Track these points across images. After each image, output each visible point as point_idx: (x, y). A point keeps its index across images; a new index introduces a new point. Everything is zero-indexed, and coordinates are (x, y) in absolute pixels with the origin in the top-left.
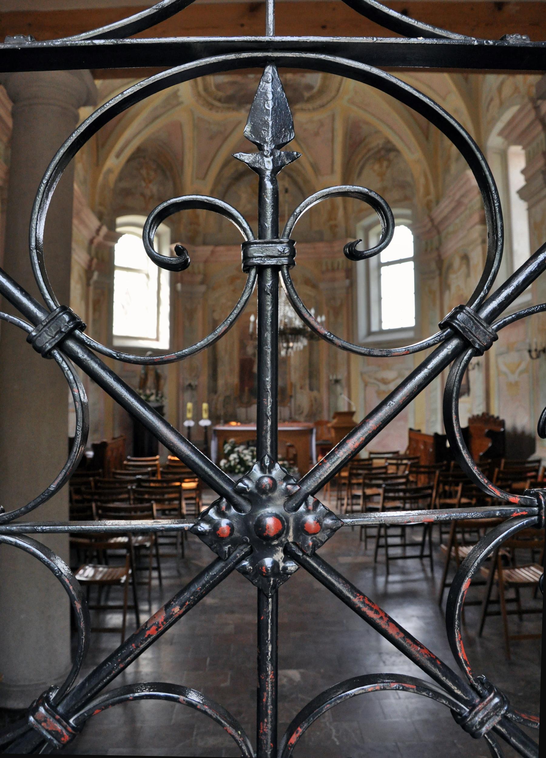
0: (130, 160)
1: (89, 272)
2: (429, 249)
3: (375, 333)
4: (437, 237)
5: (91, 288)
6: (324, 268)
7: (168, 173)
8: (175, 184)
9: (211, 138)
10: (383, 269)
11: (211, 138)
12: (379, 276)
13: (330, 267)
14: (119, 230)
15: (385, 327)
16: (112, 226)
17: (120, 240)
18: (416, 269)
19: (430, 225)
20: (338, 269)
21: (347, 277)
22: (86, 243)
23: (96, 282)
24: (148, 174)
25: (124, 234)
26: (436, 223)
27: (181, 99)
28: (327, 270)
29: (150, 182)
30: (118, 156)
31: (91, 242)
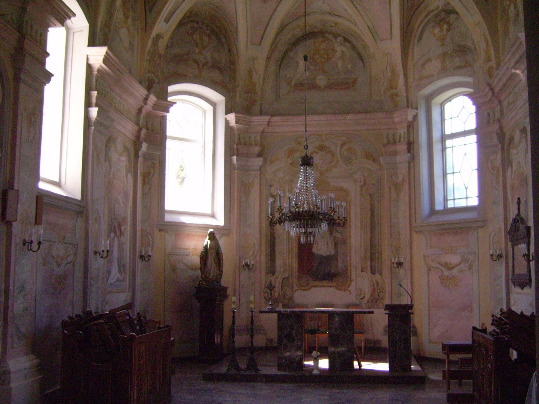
1: (137, 142)
2: (491, 121)
3: (439, 212)
4: (498, 109)
5: (140, 159)
6: (385, 141)
7: (223, 40)
8: (229, 50)
12: (444, 149)
13: (391, 141)
14: (169, 99)
15: (450, 205)
16: (163, 95)
17: (172, 109)
18: (479, 142)
19: (490, 94)
20: (400, 142)
21: (409, 151)
22: (134, 113)
23: (145, 154)
24: (201, 39)
25: (175, 103)
26: (497, 90)
28: (389, 142)
29: (204, 48)
30: (167, 21)
31: (140, 111)
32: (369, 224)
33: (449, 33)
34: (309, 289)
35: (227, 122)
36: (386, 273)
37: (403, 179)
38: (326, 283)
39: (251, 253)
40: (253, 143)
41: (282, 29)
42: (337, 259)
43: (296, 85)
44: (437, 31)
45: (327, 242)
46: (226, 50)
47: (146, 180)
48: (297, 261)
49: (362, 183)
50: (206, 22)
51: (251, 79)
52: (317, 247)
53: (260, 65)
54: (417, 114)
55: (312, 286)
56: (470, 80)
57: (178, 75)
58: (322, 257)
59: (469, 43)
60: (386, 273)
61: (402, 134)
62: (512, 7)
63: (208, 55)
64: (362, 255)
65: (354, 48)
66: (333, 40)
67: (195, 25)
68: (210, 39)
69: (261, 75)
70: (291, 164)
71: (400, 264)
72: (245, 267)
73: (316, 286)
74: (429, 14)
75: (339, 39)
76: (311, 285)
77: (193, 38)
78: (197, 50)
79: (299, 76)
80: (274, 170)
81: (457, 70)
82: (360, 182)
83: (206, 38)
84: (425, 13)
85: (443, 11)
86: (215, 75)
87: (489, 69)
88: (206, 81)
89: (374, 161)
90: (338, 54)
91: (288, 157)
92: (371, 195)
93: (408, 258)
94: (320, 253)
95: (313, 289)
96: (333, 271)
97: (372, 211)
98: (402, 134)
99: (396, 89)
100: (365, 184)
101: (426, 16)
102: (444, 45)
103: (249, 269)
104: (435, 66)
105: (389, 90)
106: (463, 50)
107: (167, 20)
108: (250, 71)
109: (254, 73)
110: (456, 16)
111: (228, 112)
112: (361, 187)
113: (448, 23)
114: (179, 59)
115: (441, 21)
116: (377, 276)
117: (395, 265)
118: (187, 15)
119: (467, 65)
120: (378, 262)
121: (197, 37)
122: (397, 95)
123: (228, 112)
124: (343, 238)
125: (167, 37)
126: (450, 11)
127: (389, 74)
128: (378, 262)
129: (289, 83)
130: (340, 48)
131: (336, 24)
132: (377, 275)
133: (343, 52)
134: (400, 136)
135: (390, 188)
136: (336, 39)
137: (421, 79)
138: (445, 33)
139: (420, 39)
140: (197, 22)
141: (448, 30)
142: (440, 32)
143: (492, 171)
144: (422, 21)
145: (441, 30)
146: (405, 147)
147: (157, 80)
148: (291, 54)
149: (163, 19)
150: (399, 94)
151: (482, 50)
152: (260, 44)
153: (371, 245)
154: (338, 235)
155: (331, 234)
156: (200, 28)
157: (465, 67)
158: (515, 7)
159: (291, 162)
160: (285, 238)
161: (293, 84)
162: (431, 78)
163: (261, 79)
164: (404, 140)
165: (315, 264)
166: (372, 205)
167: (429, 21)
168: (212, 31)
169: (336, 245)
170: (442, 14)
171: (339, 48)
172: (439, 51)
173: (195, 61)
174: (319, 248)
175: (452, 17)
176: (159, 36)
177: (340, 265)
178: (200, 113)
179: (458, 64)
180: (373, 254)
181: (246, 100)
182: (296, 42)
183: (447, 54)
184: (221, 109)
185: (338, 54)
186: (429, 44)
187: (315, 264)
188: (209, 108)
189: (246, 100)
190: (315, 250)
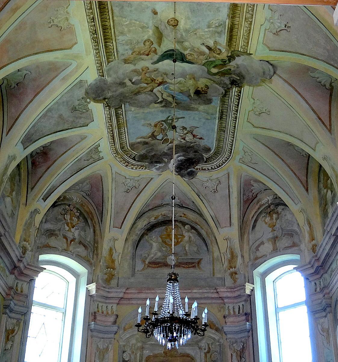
0: (54, 205)
2: (318, 290)
7: (89, 221)
8: (94, 232)
9: (127, 192)
10: (281, 314)
11: (127, 192)
24: (71, 219)
27: (101, 155)
30: (45, 199)
33: (278, 220)
35: (88, 291)
37: (243, 346)
40: (110, 312)
41: (140, 216)
43: (150, 263)
44: (268, 219)
46: (92, 230)
47: (10, 336)
50: (77, 206)
51: (112, 256)
53: (119, 245)
54: (254, 288)
56: (297, 257)
57: (50, 247)
59: (295, 228)
61: (241, 306)
62: (329, 192)
63: (76, 233)
65: (200, 234)
66: (182, 227)
67: (67, 207)
68: (78, 221)
69: (120, 253)
74: (261, 206)
75: (187, 227)
77: (64, 218)
78: (67, 228)
79: (152, 255)
81: (286, 250)
83: (75, 219)
84: (257, 207)
85: (272, 204)
86: (81, 250)
87: (313, 247)
88: (73, 255)
89: (217, 330)
90: (186, 238)
98: (241, 306)
99: (235, 268)
100: (208, 352)
101: (259, 209)
102: (275, 231)
104: (268, 247)
105: (230, 270)
106: (291, 234)
107: (45, 198)
108: (111, 250)
109: (114, 251)
110: (282, 207)
111: (89, 282)
113: (277, 213)
114: (51, 233)
115: (271, 212)
118: (61, 199)
119: (294, 245)
121: (68, 217)
122: (236, 273)
123: (89, 282)
125: (43, 212)
126: (279, 203)
127: (229, 256)
129: (144, 262)
130: (187, 235)
131: (184, 214)
133: (190, 237)
136: (184, 227)
137: (256, 259)
138: (274, 221)
139: (254, 227)
140: (69, 205)
141: (277, 219)
142: (270, 220)
143: (322, 333)
144: (256, 212)
145: (272, 219)
146: (244, 318)
147: (30, 249)
148: (146, 237)
149: (42, 197)
150: (238, 273)
151: (306, 232)
152: (121, 228)
156: (72, 210)
157: (293, 247)
158: (332, 191)
161: (147, 263)
162: (265, 258)
163: (120, 256)
164: (243, 311)
167: (261, 213)
168: (81, 213)
170: (271, 207)
171: (186, 234)
172: (271, 235)
173: (65, 237)
175: (280, 209)
176: (36, 211)
178: (64, 283)
179: (286, 245)
181: (106, 274)
182: (151, 228)
183: (277, 237)
184: (84, 280)
185: (186, 238)
186: (263, 229)
188: (72, 279)
189: (106, 274)
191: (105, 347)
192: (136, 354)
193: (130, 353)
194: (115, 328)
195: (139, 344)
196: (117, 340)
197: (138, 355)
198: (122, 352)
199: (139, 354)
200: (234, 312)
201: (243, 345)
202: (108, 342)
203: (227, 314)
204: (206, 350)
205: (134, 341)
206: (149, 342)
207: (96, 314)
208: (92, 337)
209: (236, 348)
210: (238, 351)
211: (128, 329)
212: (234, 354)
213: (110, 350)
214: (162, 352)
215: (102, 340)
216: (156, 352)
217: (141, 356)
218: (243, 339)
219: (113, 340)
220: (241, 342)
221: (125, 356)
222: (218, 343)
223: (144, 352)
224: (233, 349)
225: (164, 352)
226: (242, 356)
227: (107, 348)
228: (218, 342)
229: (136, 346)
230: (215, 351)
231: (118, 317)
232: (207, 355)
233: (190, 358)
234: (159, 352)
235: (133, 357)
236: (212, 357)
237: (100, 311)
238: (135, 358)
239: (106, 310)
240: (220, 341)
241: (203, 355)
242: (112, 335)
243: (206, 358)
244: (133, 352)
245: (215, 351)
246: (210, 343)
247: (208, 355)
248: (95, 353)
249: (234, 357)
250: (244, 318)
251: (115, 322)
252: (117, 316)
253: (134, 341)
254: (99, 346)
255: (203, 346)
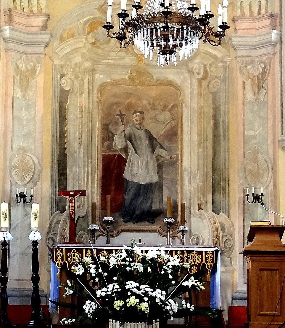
32: (210, 137)
34: (118, 234)
36: (236, 211)
38: (145, 225)
39: (28, 179)
40: (35, 9)
42: (161, 189)
45: (147, 163)
48: (100, 191)
49: (200, 76)
52: (131, 170)
55: (123, 231)
58: (139, 185)
60: (236, 211)
64: (200, 184)
70: (93, 44)
71: (257, 198)
72: (19, 198)
73: (129, 231)
76: (120, 229)
80: (66, 51)
82: (199, 73)
91: (89, 33)
92: (214, 95)
93: (271, 187)
94: (136, 180)
95: (124, 234)
96: (155, 206)
97: (215, 117)
100: (205, 77)
103: (25, 202)
112: (200, 81)
116: (223, 216)
117: (251, 198)
120: (224, 194)
124: (171, 158)
128: (224, 194)
132: (221, 213)
134: (260, 6)
135: (244, 83)
146: (268, 22)
153: (215, 169)
154: (163, 153)
155: (153, 151)
159: (93, 41)
160: (82, 155)
164: (266, 12)
165: (128, 197)
166: (216, 110)
169: (160, 167)
174: (135, 172)
177: (165, 199)
180: (217, 183)
187: (128, 197)
190: (127, 175)
191: (29, 68)
192: (82, 80)
193: (72, 77)
194: (45, 37)
195: (88, 64)
196: (50, 57)
197: (86, 81)
198: (59, 76)
199: (87, 79)
200: (251, 11)
201: (265, 67)
202: (34, 60)
203: (238, 14)
204: (202, 74)
205: (78, 59)
206: (103, 61)
207: (12, 13)
208: (6, 50)
209: (252, 73)
210: (254, 76)
211: (68, 39)
212: (248, 83)
213: (38, 72)
214: (127, 77)
215: (24, 56)
216: (116, 77)
217: (91, 83)
218: (264, 58)
219: (43, 56)
220: (261, 62)
221: (63, 82)
222: (221, 64)
223: (97, 76)
224: (247, 74)
225: (129, 78)
226: (261, 85)
227: (33, 71)
228: (222, 62)
229: (82, 67)
230: (216, 77)
231: (50, 18)
232: (202, 84)
233: (173, 88)
234: (122, 77)
235: (77, 84)
236: (211, 86)
237: (19, 8)
238: (81, 86)
239: (29, 6)
240: (225, 60)
241: (195, 84)
242: (41, 49)
243: (201, 88)
244: (77, 77)
245: (216, 77)
246: (208, 63)
247: (204, 83)
248: (14, 77)
249: (248, 87)
250: (268, 22)
251: (45, 27)
252: (48, 16)
253: (78, 59)
254: (20, 66)
255: (195, 68)
